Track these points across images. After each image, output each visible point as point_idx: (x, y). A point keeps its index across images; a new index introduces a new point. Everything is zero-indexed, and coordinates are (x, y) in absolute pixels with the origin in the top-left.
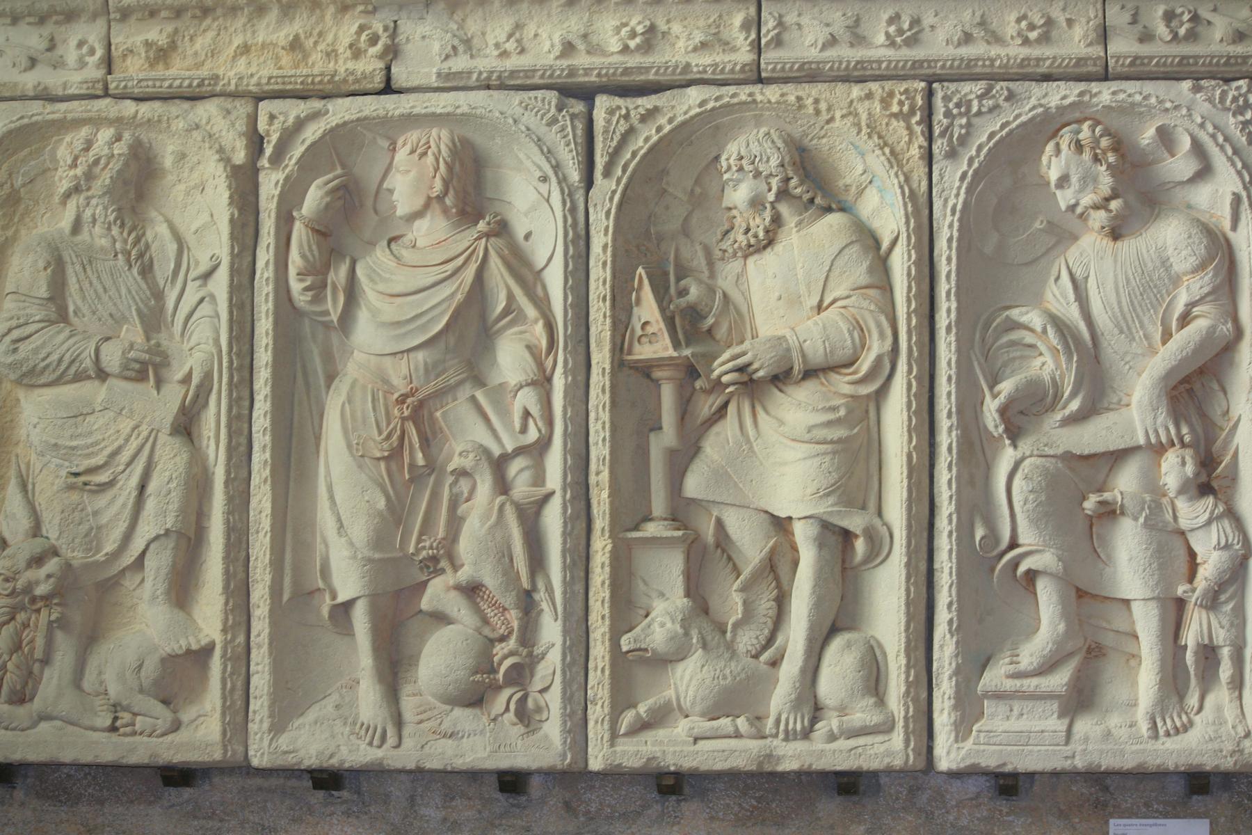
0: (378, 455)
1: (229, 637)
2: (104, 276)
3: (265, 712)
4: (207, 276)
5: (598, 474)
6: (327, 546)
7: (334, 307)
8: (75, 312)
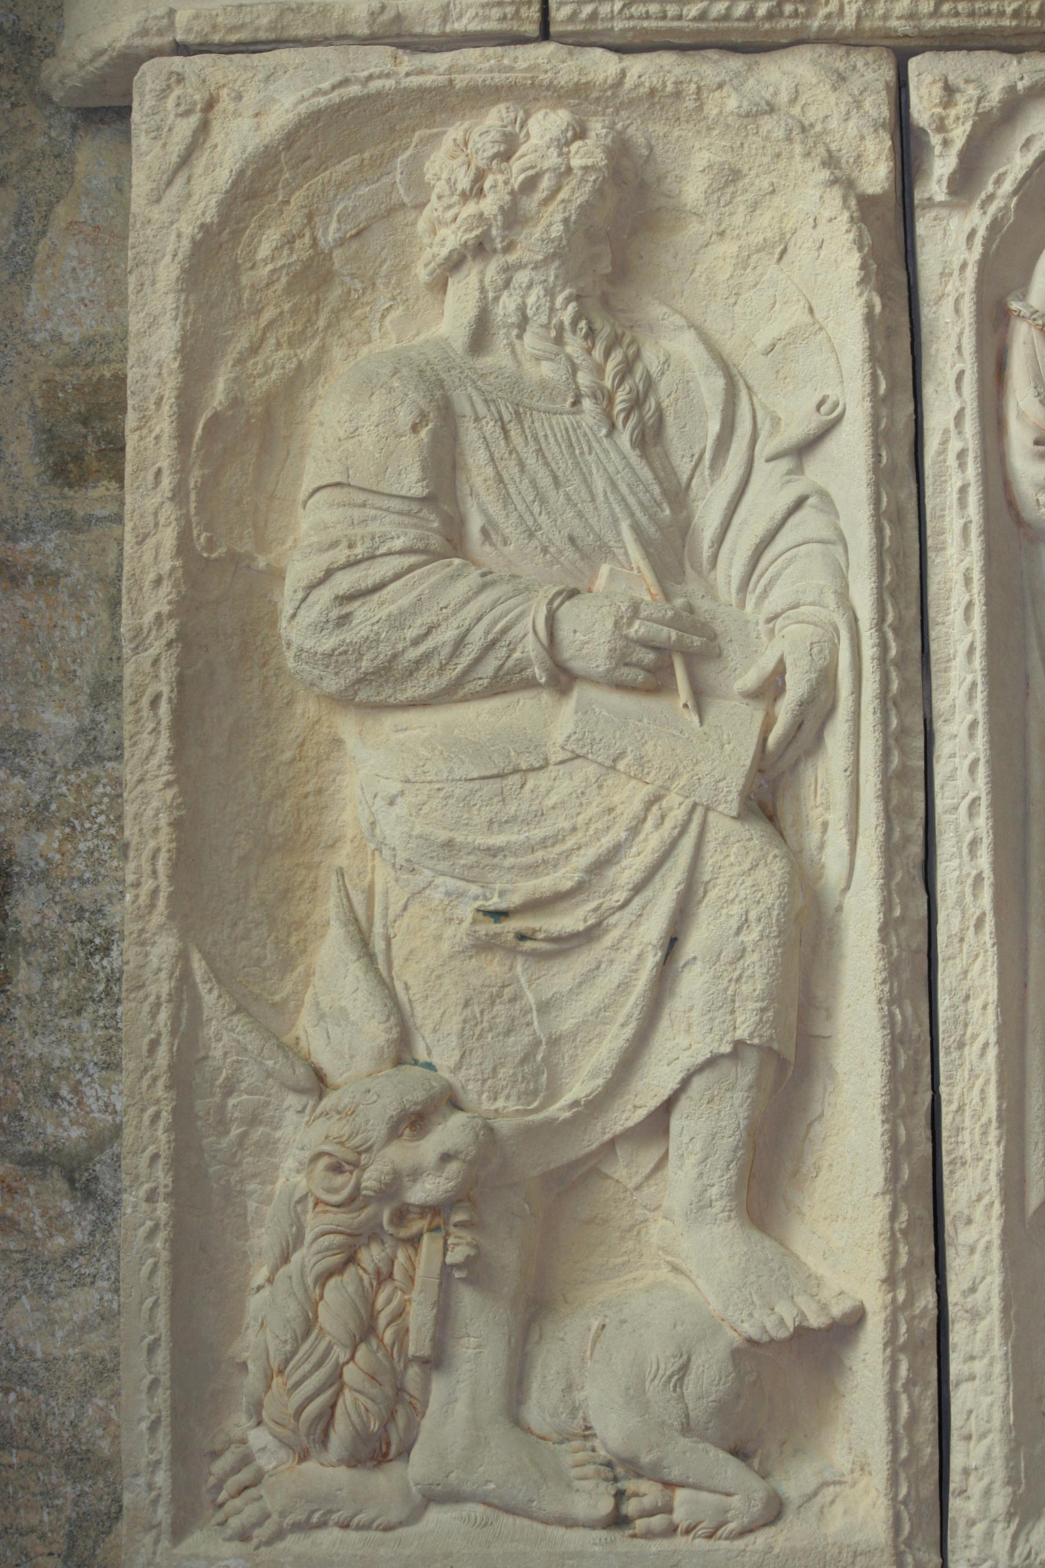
1: (901, 1296)
2: (552, 450)
3: (998, 1471)
4: (803, 450)
8: (484, 532)
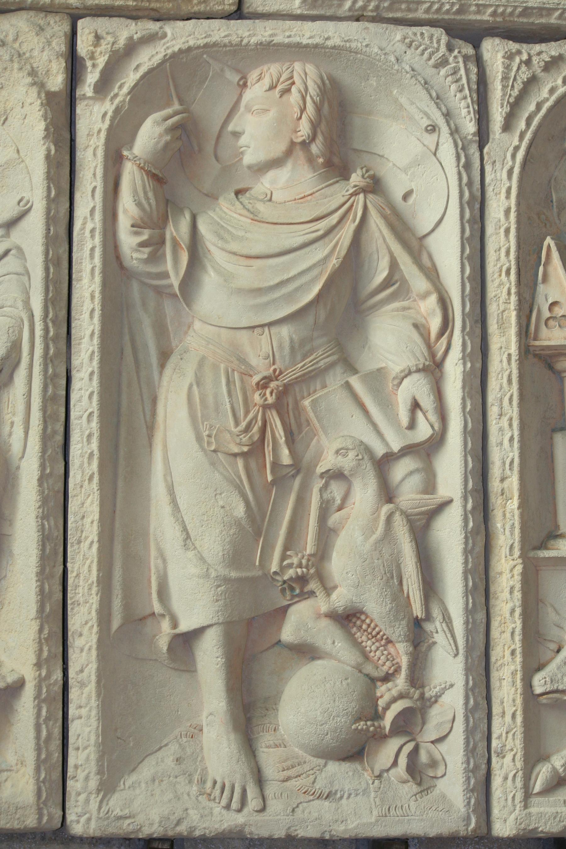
0: (236, 450)
1: (44, 673)
3: (93, 767)
5: (502, 480)
6: (164, 561)
7: (174, 270)
